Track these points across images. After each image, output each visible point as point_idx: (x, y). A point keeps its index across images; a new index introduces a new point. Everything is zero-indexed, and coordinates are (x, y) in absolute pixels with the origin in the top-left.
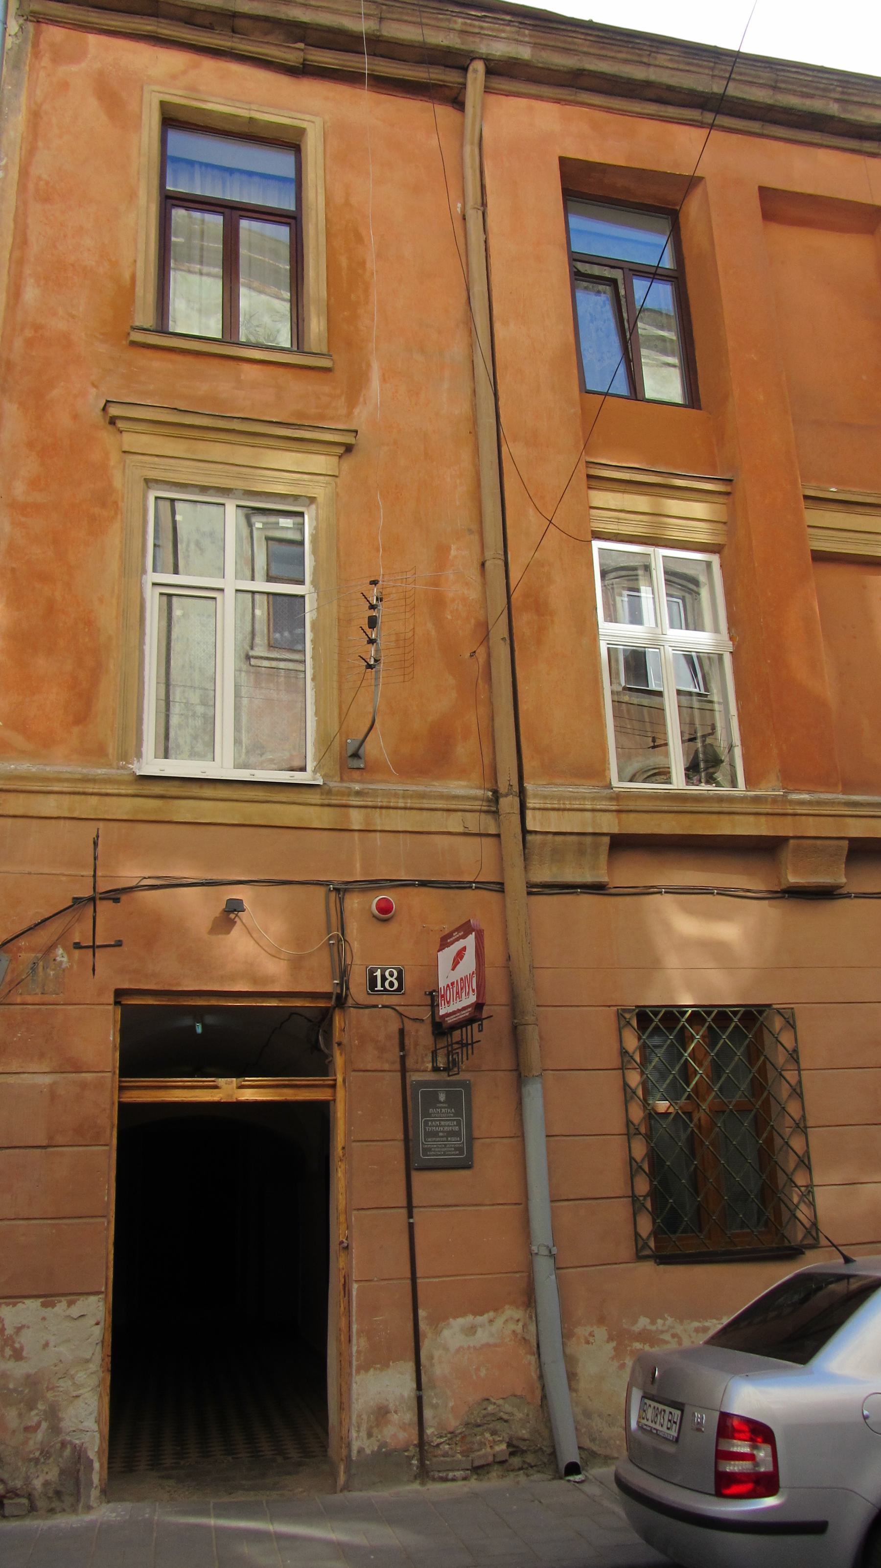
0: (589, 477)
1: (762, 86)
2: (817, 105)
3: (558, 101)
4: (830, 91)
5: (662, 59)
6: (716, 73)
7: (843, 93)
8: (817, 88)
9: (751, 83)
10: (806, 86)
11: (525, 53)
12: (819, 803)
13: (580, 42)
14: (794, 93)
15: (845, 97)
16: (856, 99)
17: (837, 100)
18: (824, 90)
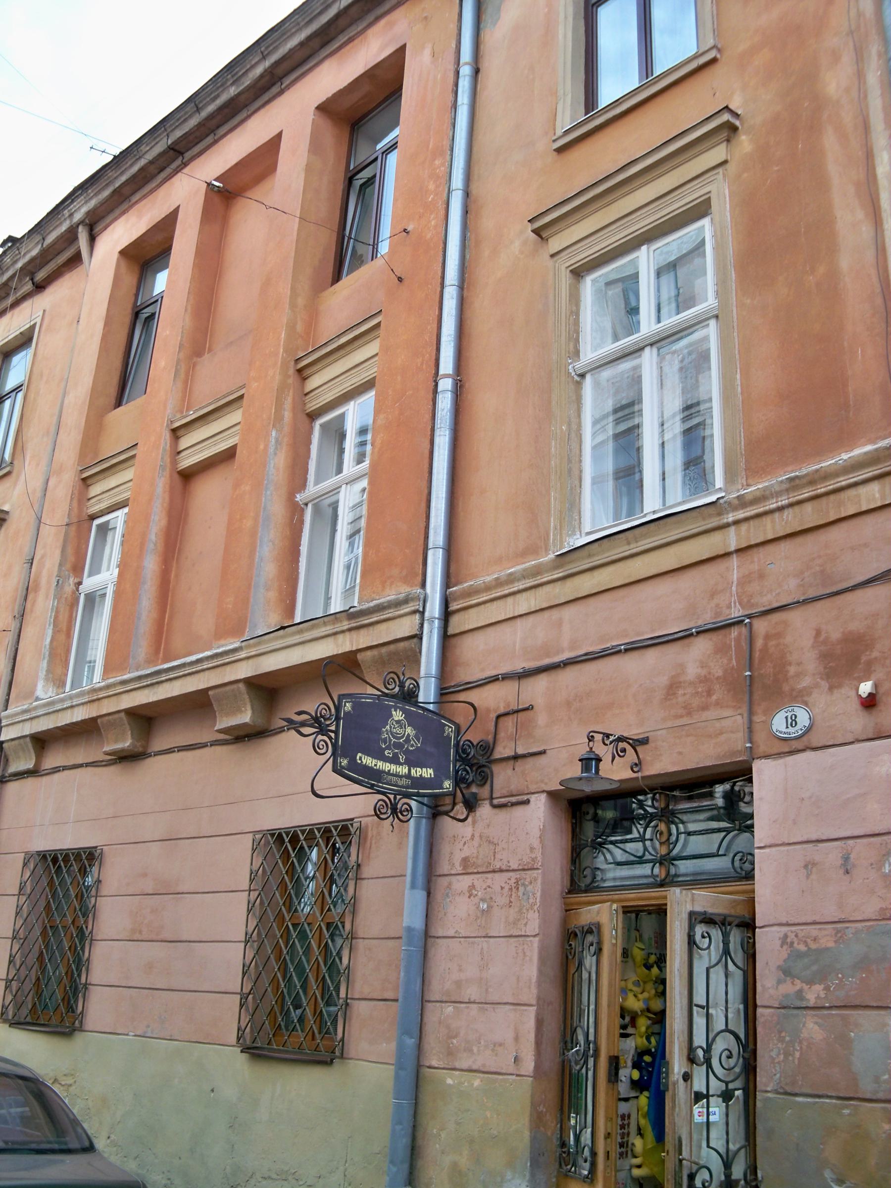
0: (84, 480)
1: (191, 116)
2: (224, 98)
3: (123, 213)
4: (226, 82)
5: (144, 148)
6: (169, 130)
7: (233, 76)
8: (218, 88)
9: (185, 120)
10: (211, 93)
11: (92, 203)
13: (111, 174)
14: (208, 103)
15: (235, 78)
16: (240, 73)
17: (232, 84)
18: (222, 85)
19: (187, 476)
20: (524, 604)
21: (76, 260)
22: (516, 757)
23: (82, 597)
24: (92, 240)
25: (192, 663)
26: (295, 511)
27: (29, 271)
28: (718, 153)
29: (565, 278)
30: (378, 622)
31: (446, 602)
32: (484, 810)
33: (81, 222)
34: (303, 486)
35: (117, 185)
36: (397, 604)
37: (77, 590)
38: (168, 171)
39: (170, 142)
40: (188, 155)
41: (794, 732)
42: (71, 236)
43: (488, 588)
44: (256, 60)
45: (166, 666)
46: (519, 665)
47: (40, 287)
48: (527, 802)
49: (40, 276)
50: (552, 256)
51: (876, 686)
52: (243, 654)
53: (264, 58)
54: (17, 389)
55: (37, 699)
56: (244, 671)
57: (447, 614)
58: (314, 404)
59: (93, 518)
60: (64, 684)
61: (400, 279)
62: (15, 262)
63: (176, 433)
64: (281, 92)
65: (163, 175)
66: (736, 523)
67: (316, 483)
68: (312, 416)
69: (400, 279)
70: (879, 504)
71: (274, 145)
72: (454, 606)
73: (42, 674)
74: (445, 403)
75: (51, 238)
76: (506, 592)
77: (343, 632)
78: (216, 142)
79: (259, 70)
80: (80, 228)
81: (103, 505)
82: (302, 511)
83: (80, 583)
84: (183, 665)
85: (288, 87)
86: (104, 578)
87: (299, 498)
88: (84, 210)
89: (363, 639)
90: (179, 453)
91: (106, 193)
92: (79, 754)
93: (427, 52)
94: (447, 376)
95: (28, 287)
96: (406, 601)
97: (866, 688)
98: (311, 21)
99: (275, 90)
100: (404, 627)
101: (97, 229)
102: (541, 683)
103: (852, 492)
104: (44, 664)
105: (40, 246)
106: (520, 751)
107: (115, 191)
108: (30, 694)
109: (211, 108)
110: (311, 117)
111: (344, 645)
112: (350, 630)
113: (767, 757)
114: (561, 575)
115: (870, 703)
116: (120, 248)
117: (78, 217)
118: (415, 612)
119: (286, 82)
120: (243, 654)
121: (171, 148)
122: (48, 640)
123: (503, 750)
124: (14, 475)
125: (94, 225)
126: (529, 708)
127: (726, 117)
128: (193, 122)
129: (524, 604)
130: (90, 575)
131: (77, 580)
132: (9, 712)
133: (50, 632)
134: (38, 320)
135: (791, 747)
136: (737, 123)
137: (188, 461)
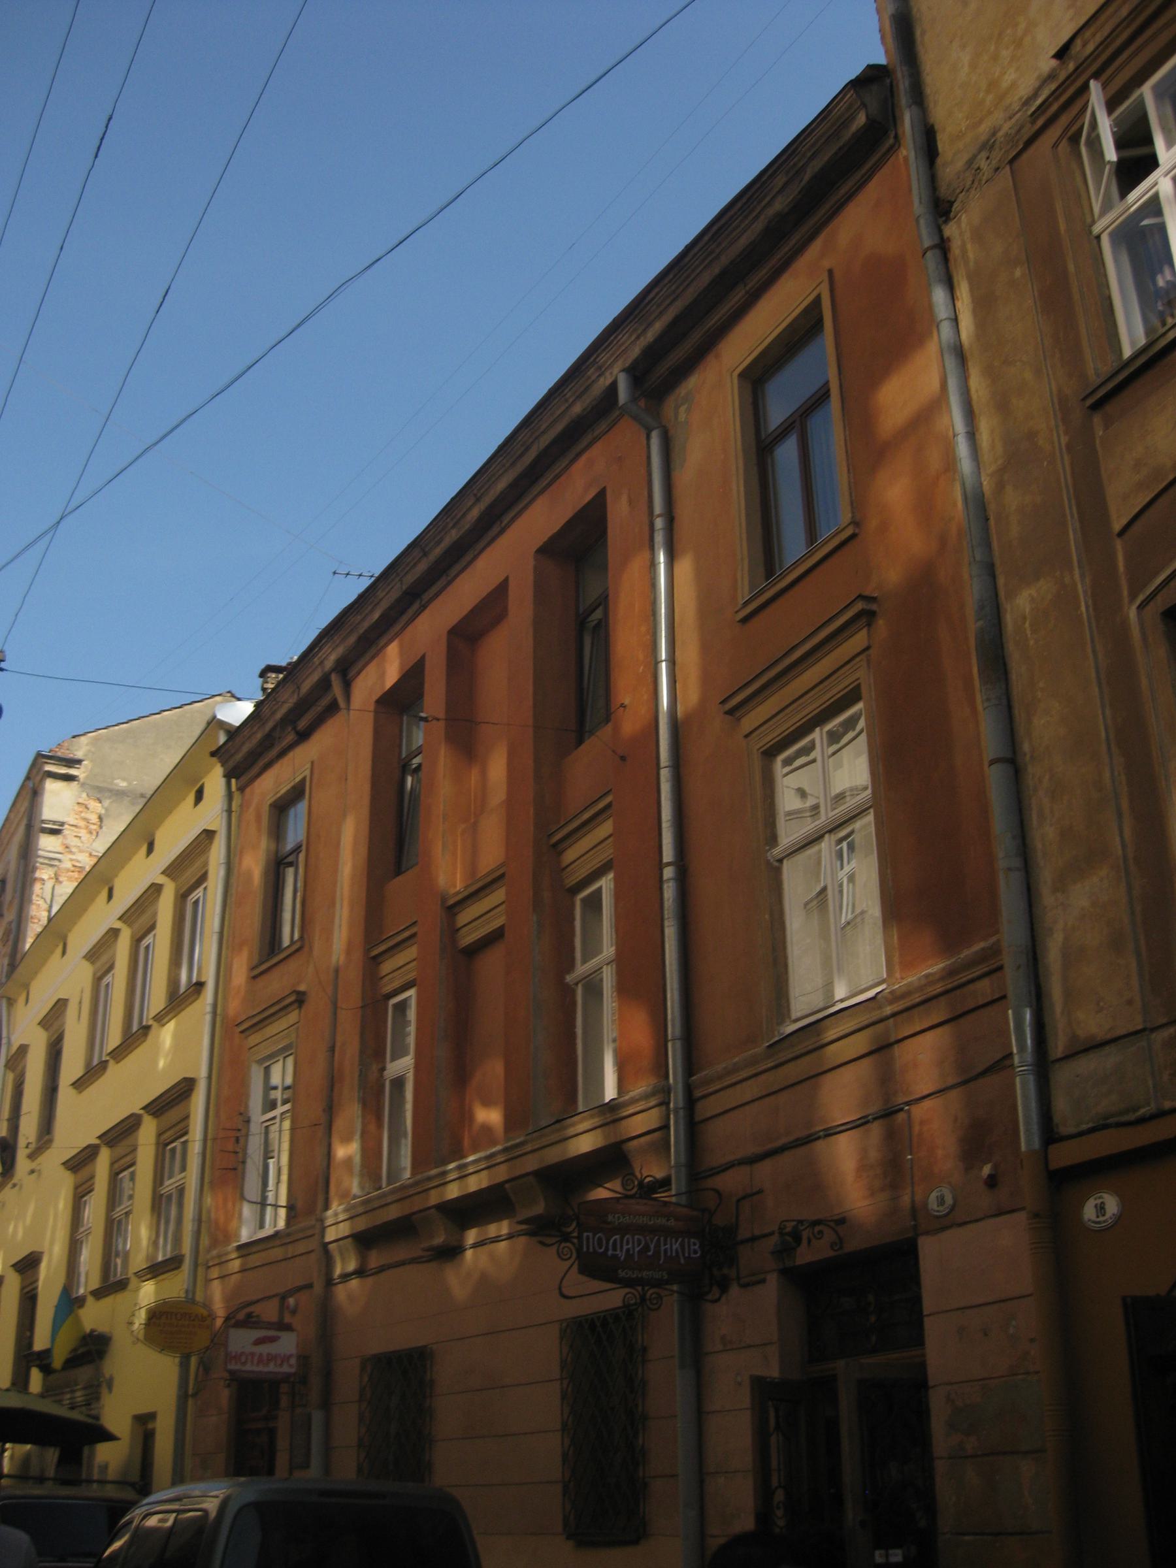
1: (419, 561)
5: (381, 594)
11: (340, 651)
20: (749, 1090)
22: (754, 1239)
23: (387, 1084)
24: (347, 685)
26: (567, 992)
27: (291, 719)
28: (859, 639)
29: (757, 762)
31: (689, 1090)
32: (734, 1290)
33: (333, 670)
34: (571, 967)
35: (361, 631)
37: (382, 1076)
38: (411, 611)
39: (404, 588)
40: (426, 597)
41: (943, 1210)
42: (324, 684)
43: (720, 1078)
44: (470, 503)
46: (753, 1149)
47: (304, 736)
48: (763, 1281)
49: (302, 724)
50: (746, 736)
51: (995, 1167)
52: (529, 1148)
53: (478, 500)
54: (297, 849)
57: (691, 1102)
58: (571, 881)
60: (379, 1178)
61: (623, 758)
62: (273, 713)
64: (502, 531)
65: (405, 618)
66: (894, 1015)
67: (584, 961)
69: (623, 758)
70: (990, 999)
71: (502, 589)
72: (698, 1093)
74: (669, 892)
75: (306, 686)
76: (734, 1080)
78: (449, 583)
79: (475, 513)
80: (333, 677)
81: (396, 984)
82: (573, 993)
83: (383, 1069)
85: (508, 526)
86: (403, 1065)
87: (569, 978)
88: (333, 657)
90: (458, 930)
91: (352, 640)
92: (402, 1251)
93: (624, 499)
94: (668, 864)
95: (291, 737)
97: (987, 1170)
98: (513, 464)
99: (496, 529)
101: (352, 673)
102: (767, 1166)
103: (971, 987)
105: (296, 696)
106: (757, 1233)
107: (360, 639)
109: (438, 551)
110: (532, 563)
113: (927, 1233)
114: (772, 1064)
115: (992, 1182)
116: (375, 698)
117: (329, 664)
119: (506, 520)
121: (406, 593)
123: (743, 1234)
124: (306, 949)
125: (346, 669)
126: (760, 1192)
127: (860, 606)
128: (423, 566)
129: (749, 1090)
130: (393, 1059)
134: (307, 773)
135: (945, 1223)
136: (874, 607)
137: (468, 938)
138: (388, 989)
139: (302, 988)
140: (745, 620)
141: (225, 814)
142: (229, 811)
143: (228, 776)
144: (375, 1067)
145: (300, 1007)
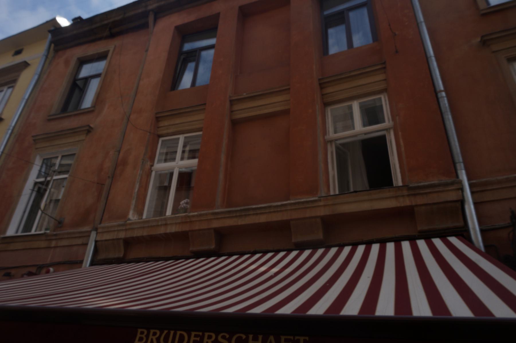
12: (201, 215)
19: (235, 124)
21: (145, 26)
23: (153, 173)
25: (303, 203)
30: (430, 193)
36: (446, 185)
37: (151, 169)
42: (145, 15)
45: (254, 207)
47: (112, 36)
50: (494, 52)
52: (321, 203)
55: (129, 220)
56: (322, 212)
59: (160, 136)
61: (397, 52)
63: (232, 102)
68: (326, 104)
69: (397, 52)
73: (132, 207)
77: (403, 196)
80: (151, 13)
83: (152, 166)
84: (270, 207)
89: (420, 200)
96: (452, 184)
100: (452, 196)
104: (134, 202)
108: (125, 216)
111: (407, 202)
112: (408, 195)
117: (150, 7)
118: (458, 189)
120: (321, 203)
122: (136, 190)
130: (158, 163)
131: (151, 164)
132: (103, 225)
133: (137, 186)
138: (161, 132)
139: (92, 126)
140: (484, 15)
141: (44, 57)
142: (47, 57)
143: (51, 43)
144: (149, 163)
145: (87, 134)
